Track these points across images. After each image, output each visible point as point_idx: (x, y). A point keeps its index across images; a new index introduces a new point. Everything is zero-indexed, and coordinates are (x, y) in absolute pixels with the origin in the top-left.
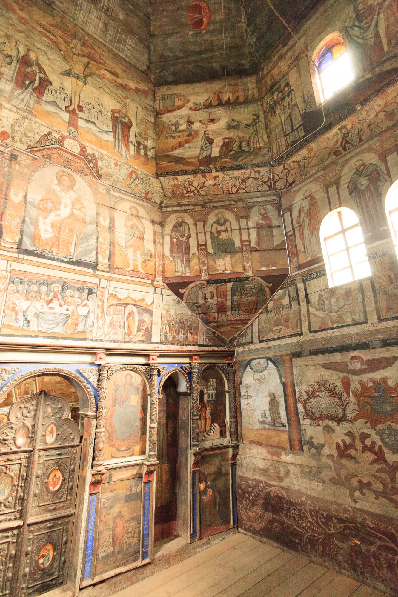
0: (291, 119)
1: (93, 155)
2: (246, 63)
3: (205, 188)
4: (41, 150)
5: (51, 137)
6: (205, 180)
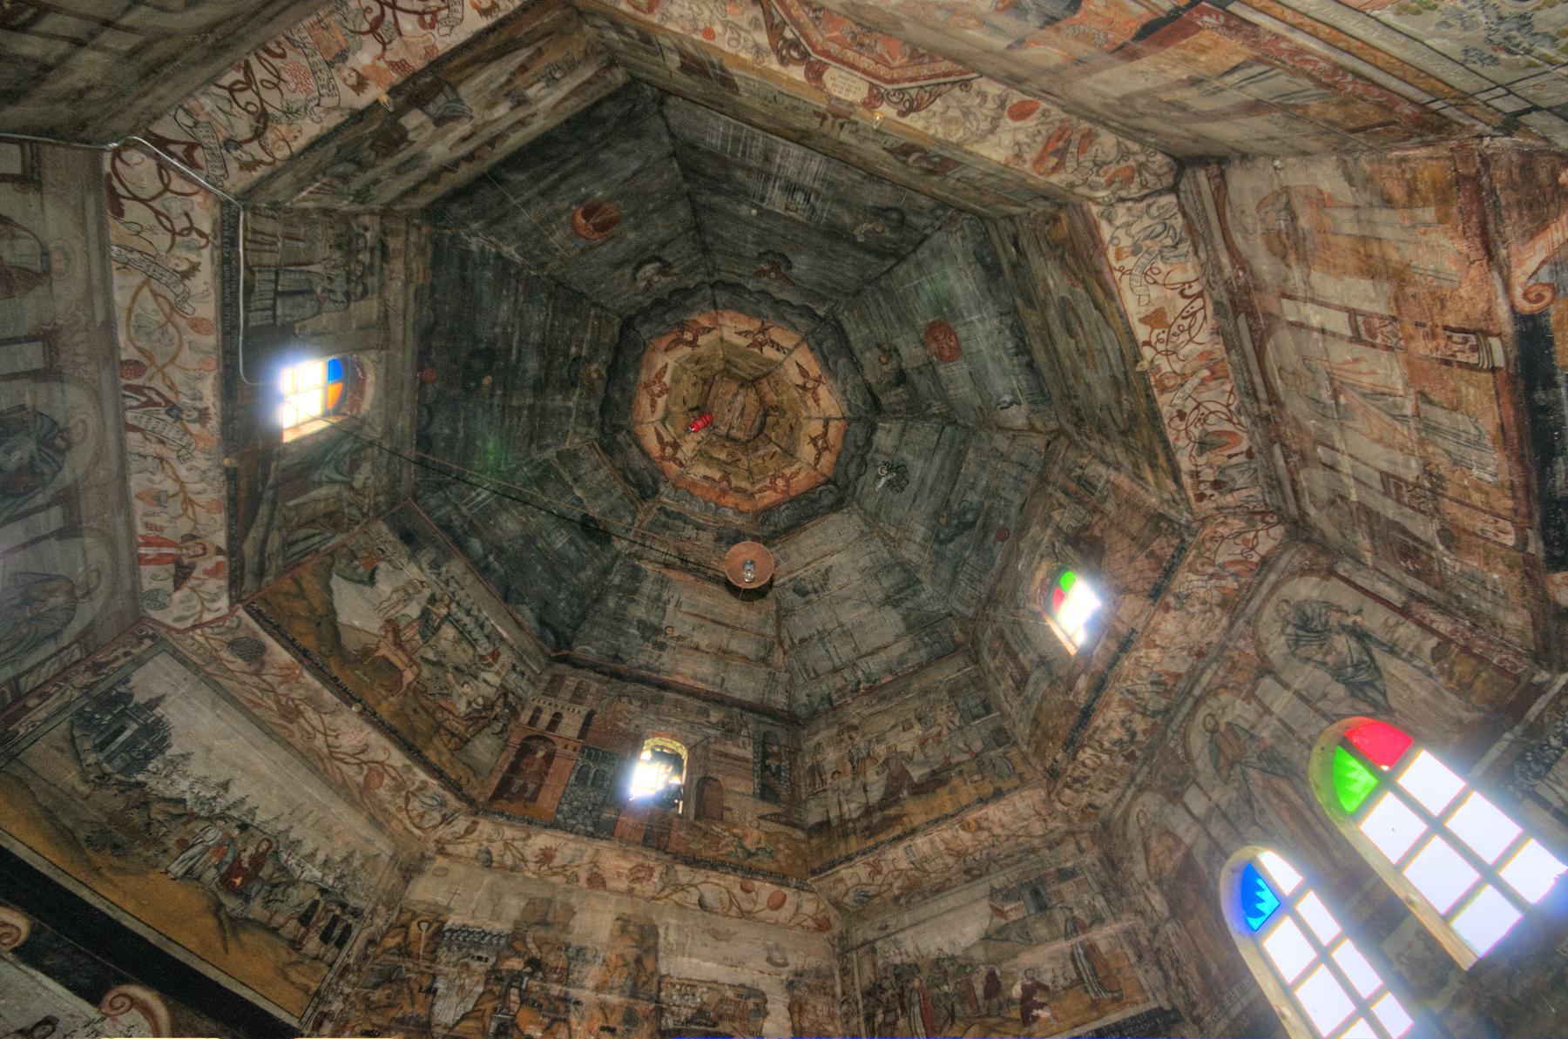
0: (301, 293)
1: (783, 61)
2: (457, 210)
3: (366, 27)
4: (936, 76)
5: (901, 107)
6: (389, 56)
